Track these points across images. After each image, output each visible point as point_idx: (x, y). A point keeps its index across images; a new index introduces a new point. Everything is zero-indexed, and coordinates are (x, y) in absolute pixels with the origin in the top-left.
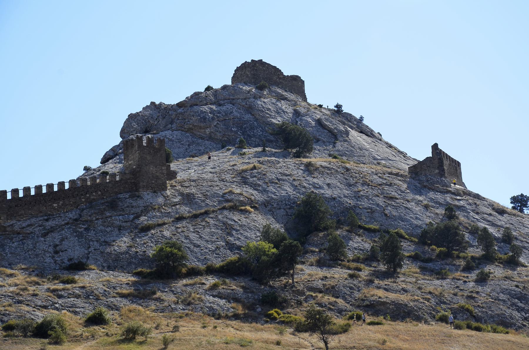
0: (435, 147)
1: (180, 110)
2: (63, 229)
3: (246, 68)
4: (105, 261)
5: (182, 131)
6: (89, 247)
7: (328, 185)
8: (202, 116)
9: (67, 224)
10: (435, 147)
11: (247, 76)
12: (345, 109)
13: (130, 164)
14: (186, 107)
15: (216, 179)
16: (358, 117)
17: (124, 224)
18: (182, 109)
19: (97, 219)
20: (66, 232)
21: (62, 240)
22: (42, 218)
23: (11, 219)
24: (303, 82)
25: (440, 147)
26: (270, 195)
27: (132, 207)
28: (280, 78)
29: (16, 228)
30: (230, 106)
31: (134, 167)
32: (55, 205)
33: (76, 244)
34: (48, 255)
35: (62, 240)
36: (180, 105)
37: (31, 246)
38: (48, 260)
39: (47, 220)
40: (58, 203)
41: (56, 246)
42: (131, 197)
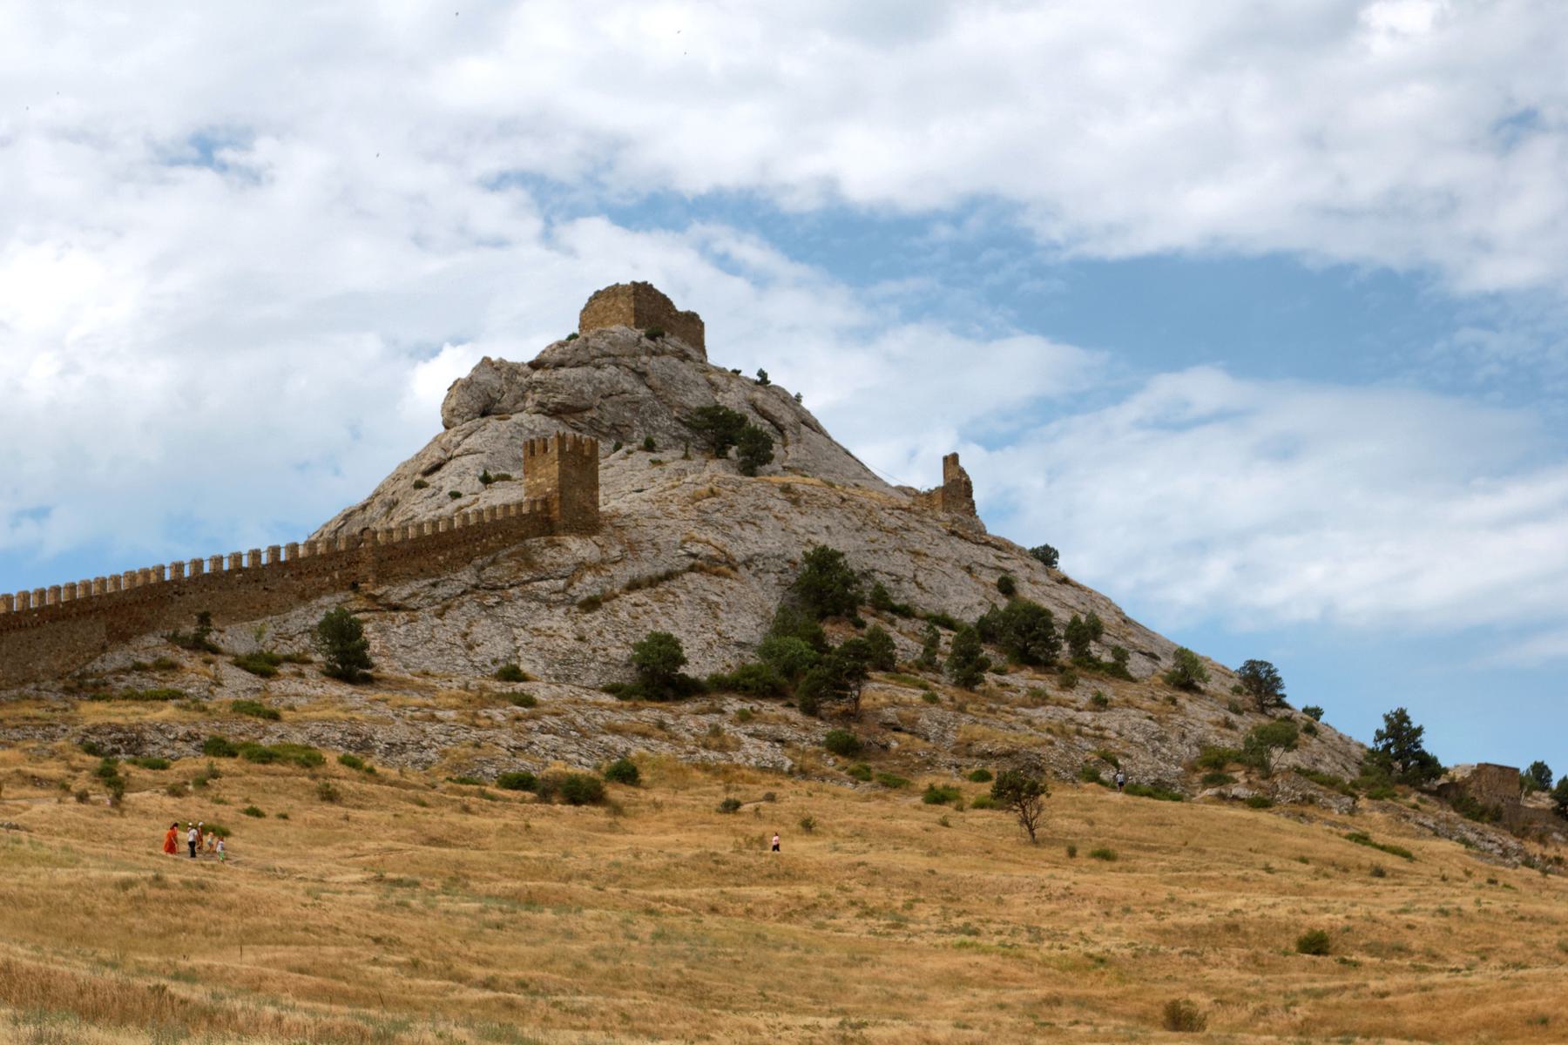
0: (951, 461)
1: (537, 375)
2: (462, 604)
3: (616, 295)
4: (548, 666)
5: (545, 414)
6: (515, 639)
7: (827, 527)
8: (577, 386)
9: (464, 593)
10: (951, 461)
11: (620, 311)
12: (774, 379)
13: (538, 485)
14: (547, 368)
15: (658, 513)
16: (793, 395)
17: (553, 597)
18: (539, 372)
19: (511, 586)
20: (471, 608)
21: (470, 625)
22: (425, 582)
23: (383, 584)
24: (702, 325)
25: (962, 463)
26: (749, 545)
27: (559, 565)
28: (671, 317)
29: (394, 599)
30: (612, 369)
31: (548, 490)
32: (440, 558)
33: (493, 631)
34: (458, 651)
35: (470, 625)
36: (535, 365)
37: (427, 635)
38: (461, 661)
39: (434, 585)
40: (445, 555)
41: (465, 635)
42: (552, 544)
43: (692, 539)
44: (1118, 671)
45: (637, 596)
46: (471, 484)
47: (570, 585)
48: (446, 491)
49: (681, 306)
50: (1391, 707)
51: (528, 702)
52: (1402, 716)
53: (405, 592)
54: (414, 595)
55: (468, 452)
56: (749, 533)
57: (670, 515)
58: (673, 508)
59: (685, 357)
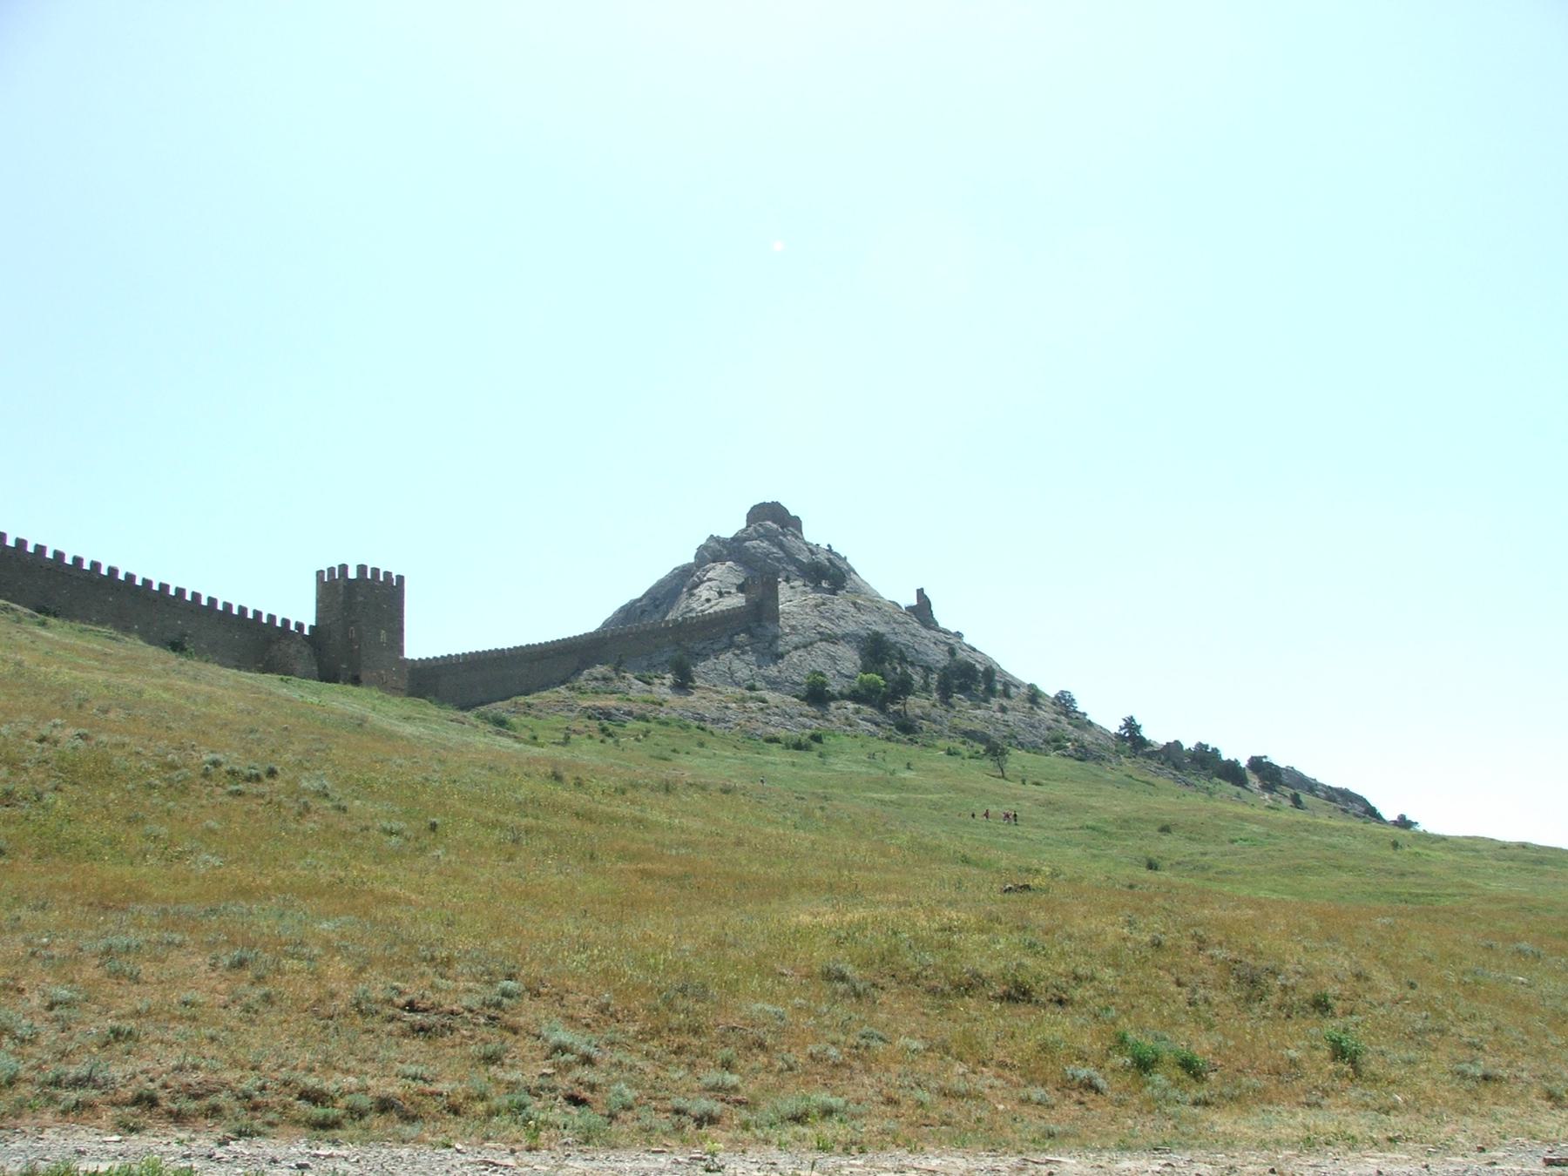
0: (920, 592)
10: (920, 592)
12: (835, 549)
42: (760, 626)
43: (819, 625)
44: (1006, 694)
45: (800, 652)
46: (713, 594)
47: (770, 645)
48: (703, 598)
49: (792, 513)
50: (1127, 715)
51: (764, 701)
52: (1132, 719)
53: (701, 646)
54: (704, 648)
55: (709, 580)
56: (842, 623)
57: (807, 614)
58: (807, 610)
59: (797, 537)
